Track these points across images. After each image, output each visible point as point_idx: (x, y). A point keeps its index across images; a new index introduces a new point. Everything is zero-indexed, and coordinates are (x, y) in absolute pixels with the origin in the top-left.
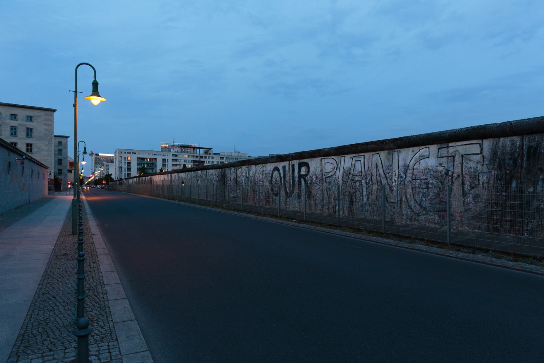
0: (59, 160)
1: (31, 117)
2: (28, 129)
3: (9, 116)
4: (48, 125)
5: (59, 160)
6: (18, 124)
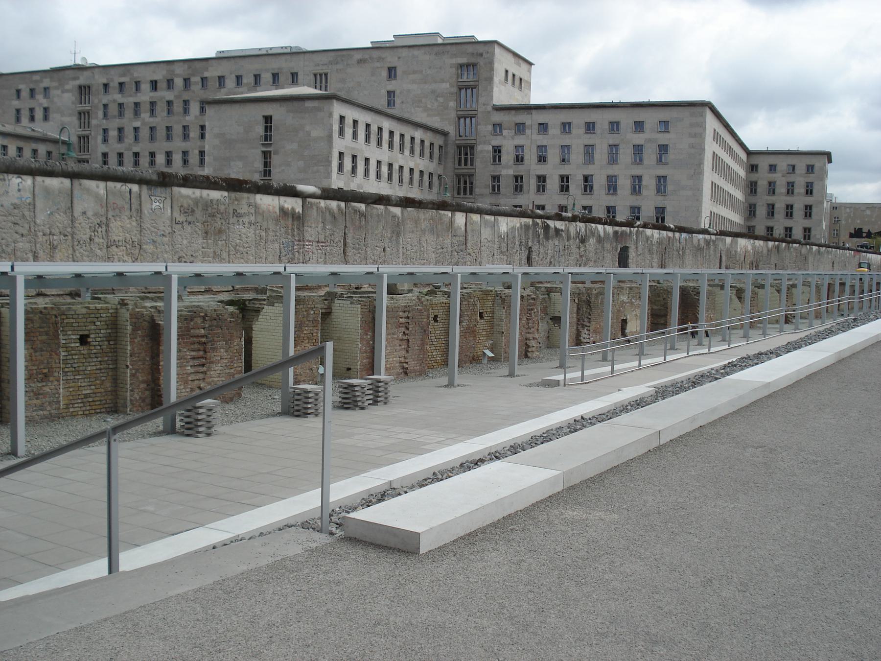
0: (806, 206)
1: (666, 123)
3: (632, 125)
4: (695, 136)
5: (806, 206)
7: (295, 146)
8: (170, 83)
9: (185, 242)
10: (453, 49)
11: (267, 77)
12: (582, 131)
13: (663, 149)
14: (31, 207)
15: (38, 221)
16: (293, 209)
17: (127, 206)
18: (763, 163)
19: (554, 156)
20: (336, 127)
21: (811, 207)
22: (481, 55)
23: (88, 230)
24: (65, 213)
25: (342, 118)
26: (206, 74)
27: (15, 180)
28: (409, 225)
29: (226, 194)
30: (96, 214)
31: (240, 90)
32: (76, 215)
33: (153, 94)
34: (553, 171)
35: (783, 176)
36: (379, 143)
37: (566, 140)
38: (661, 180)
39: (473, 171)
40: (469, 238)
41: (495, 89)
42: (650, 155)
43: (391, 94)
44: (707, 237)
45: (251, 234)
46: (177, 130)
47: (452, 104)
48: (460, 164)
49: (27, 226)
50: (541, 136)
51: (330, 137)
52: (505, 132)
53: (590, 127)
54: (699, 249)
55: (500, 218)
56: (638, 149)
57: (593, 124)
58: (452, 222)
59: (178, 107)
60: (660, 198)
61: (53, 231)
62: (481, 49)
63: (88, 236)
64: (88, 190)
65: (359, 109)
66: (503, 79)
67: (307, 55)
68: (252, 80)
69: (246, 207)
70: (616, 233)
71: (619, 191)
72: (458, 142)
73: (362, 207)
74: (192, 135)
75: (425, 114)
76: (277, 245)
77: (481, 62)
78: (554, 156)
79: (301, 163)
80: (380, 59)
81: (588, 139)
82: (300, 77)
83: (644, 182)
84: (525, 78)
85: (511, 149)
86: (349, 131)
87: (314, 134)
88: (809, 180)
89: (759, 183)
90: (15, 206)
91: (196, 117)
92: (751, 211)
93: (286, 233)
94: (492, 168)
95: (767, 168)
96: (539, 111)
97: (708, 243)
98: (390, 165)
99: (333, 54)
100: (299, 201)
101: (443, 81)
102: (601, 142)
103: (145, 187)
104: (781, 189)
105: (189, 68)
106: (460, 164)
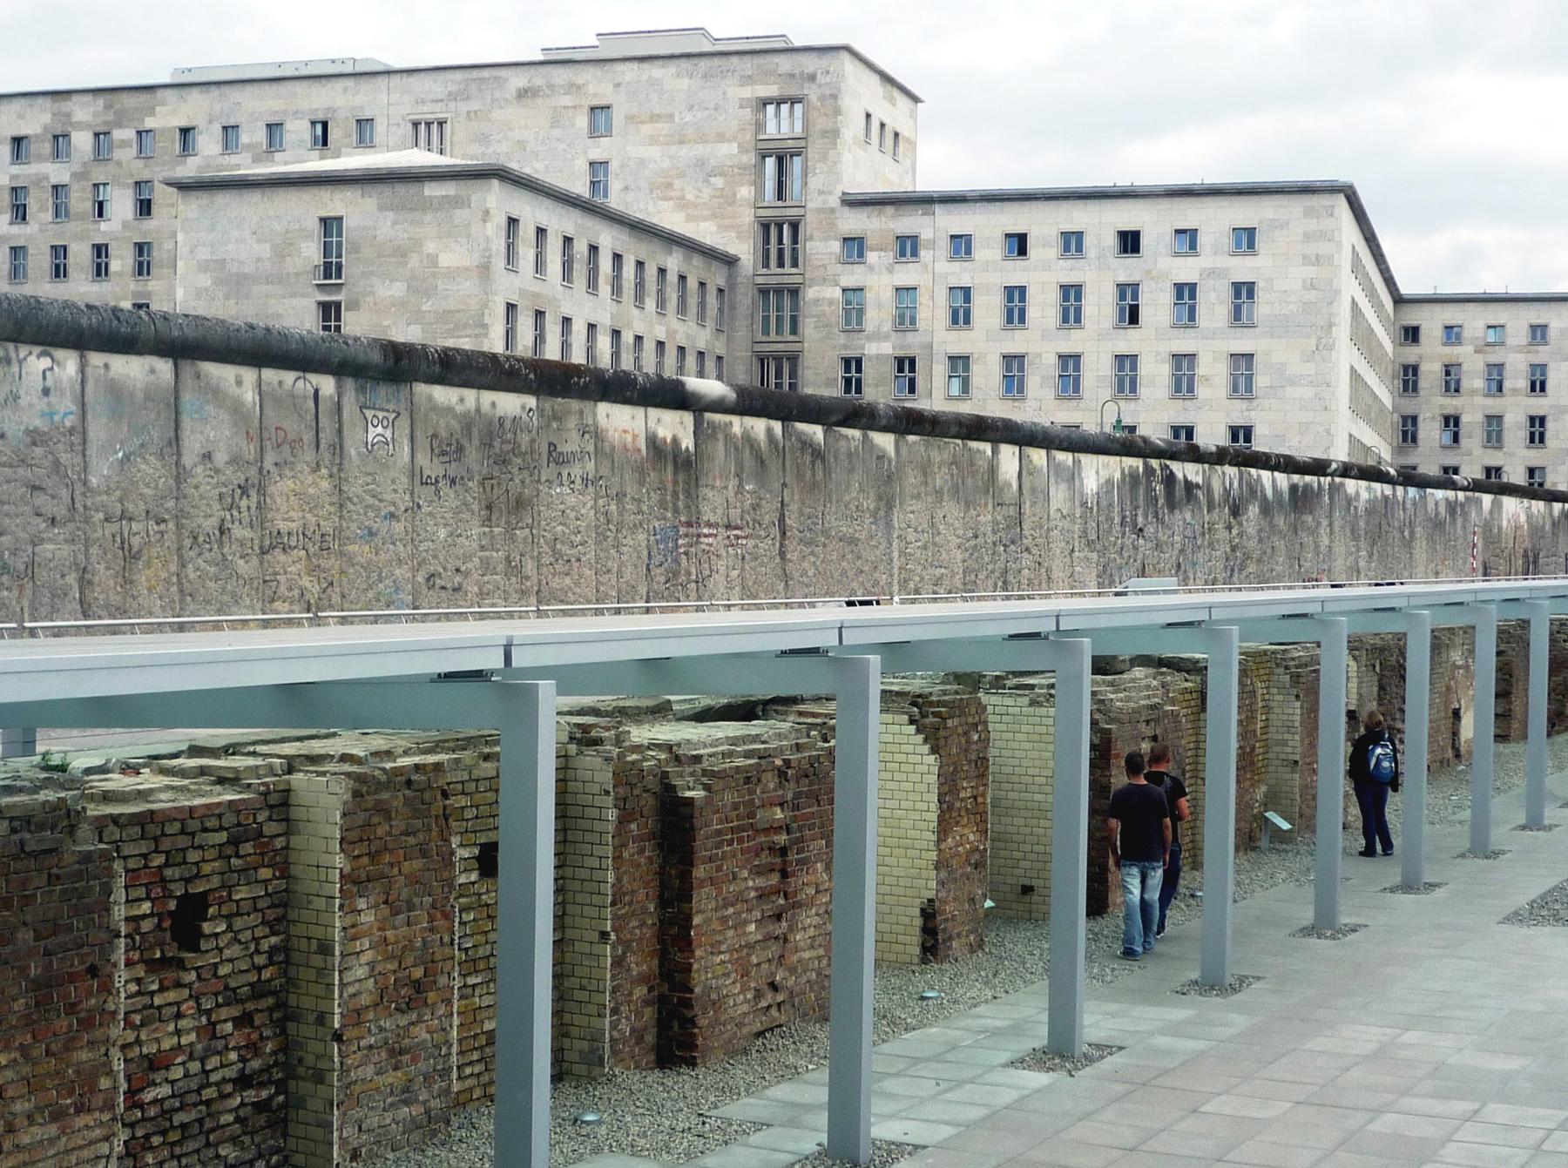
0: (1532, 419)
1: (1251, 232)
2: (1238, 288)
3: (1169, 236)
4: (1318, 260)
5: (1532, 419)
6: (1202, 271)
7: (398, 289)
8: (59, 142)
9: (442, 533)
10: (747, 65)
11: (298, 131)
12: (1053, 251)
13: (1244, 291)
14: (76, 439)
15: (94, 481)
16: (675, 440)
17: (308, 437)
18: (1431, 322)
19: (989, 309)
20: (500, 245)
21: (1542, 420)
22: (812, 78)
23: (216, 506)
24: (161, 456)
25: (512, 222)
26: (149, 123)
27: (35, 363)
28: (912, 478)
29: (531, 401)
30: (235, 460)
31: (234, 159)
32: (187, 461)
33: (15, 169)
34: (1041, 340)
35: (1476, 352)
36: (592, 284)
37: (1017, 273)
38: (1242, 361)
39: (796, 347)
40: (1027, 508)
41: (847, 157)
42: (1214, 305)
43: (597, 167)
44: (1450, 494)
45: (587, 511)
46: (80, 254)
47: (746, 192)
48: (766, 332)
49: (65, 493)
50: (956, 266)
51: (485, 269)
52: (872, 257)
53: (1072, 242)
54: (1438, 525)
55: (1088, 460)
56: (1185, 293)
57: (1079, 235)
58: (993, 470)
59: (80, 201)
60: (1239, 405)
61: (130, 507)
62: (810, 63)
63: (214, 521)
64: (215, 393)
65: (548, 203)
66: (862, 133)
67: (396, 79)
68: (261, 136)
69: (575, 435)
70: (1293, 488)
71: (1143, 391)
72: (760, 280)
73: (816, 432)
74: (115, 266)
75: (681, 216)
76: (642, 537)
77: (812, 93)
78: (989, 309)
80: (574, 88)
81: (1069, 272)
82: (380, 128)
83: (1202, 369)
84: (905, 132)
85: (888, 295)
86: (527, 253)
87: (447, 260)
88: (1537, 360)
89: (1423, 368)
90: (35, 437)
91: (125, 225)
92: (1408, 431)
93: (662, 504)
94: (842, 339)
95: (1439, 333)
96: (952, 207)
97: (1452, 507)
98: (616, 334)
99: (459, 75)
100: (688, 418)
101: (721, 138)
102: (1101, 276)
103: (349, 384)
104: (1474, 380)
105: (108, 107)
106: (766, 332)
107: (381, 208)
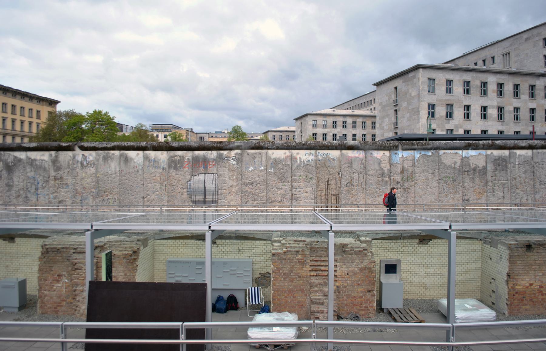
65: (451, 72)
79: (408, 114)
80: (539, 34)
107: (403, 82)
